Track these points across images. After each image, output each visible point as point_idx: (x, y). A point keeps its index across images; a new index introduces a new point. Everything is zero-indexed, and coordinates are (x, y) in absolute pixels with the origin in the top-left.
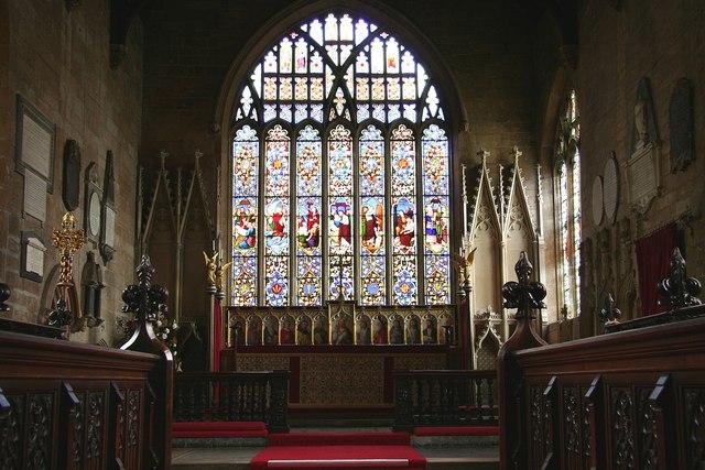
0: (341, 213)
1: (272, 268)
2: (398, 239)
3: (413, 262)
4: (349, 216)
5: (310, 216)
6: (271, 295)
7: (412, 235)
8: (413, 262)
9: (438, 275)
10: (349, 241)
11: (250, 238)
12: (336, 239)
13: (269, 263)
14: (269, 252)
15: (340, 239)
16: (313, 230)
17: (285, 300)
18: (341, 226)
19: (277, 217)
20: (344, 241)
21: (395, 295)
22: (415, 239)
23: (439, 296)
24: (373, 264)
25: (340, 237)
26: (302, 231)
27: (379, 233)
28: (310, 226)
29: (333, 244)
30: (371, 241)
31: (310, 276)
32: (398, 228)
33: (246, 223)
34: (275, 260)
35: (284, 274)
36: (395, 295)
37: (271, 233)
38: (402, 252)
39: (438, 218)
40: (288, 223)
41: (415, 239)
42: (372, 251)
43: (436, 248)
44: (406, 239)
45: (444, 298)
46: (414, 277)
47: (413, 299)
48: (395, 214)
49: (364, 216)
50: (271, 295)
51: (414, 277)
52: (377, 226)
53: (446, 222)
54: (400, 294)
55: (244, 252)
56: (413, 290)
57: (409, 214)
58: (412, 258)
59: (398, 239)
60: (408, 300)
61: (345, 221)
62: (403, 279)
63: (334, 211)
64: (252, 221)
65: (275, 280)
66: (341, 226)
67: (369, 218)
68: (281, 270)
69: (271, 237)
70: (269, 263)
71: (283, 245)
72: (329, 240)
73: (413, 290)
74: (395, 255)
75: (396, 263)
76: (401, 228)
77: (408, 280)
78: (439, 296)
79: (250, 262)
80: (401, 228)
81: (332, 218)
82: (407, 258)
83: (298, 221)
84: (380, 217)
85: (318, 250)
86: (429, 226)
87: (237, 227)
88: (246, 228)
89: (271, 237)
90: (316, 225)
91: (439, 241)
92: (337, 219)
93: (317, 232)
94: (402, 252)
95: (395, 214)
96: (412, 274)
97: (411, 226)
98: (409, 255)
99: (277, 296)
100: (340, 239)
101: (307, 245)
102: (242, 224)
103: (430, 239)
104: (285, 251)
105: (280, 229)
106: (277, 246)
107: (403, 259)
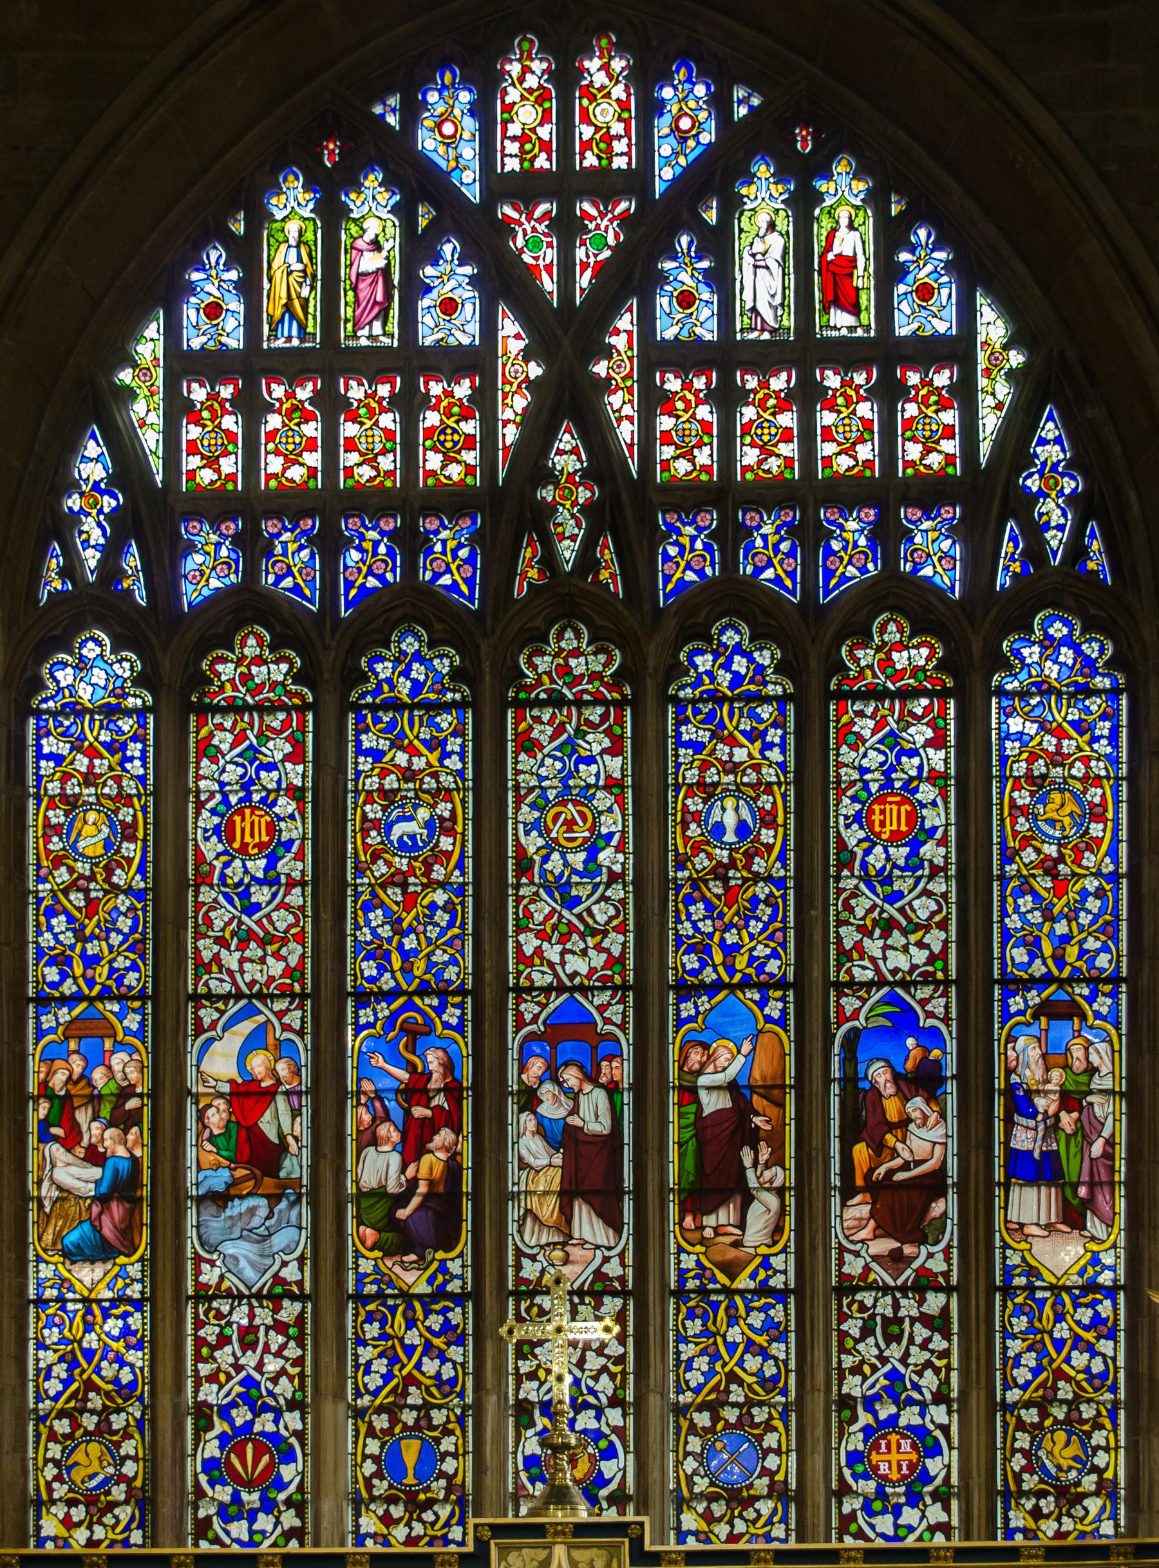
0: (571, 1077)
1: (224, 1356)
2: (858, 1209)
3: (938, 1323)
4: (612, 1089)
5: (417, 1090)
6: (224, 1494)
7: (934, 1184)
8: (938, 1323)
9: (1065, 1391)
10: (614, 1222)
11: (117, 1210)
12: (548, 1209)
13: (210, 1333)
14: (210, 1276)
15: (566, 1213)
16: (432, 1164)
17: (290, 1519)
18: (564, 1138)
19: (248, 1096)
20: (587, 1225)
21: (844, 1490)
22: (946, 1206)
23: (1069, 1497)
24: (735, 1334)
25: (567, 1196)
26: (379, 1167)
27: (767, 1176)
28: (413, 1146)
29: (532, 1237)
30: (725, 1216)
31: (415, 1397)
32: (861, 1152)
33: (92, 1130)
34: (240, 1316)
35: (285, 1388)
36: (844, 1490)
37: (219, 1180)
38: (879, 1274)
39: (1070, 1100)
40: (302, 1127)
41: (946, 1206)
42: (731, 1269)
43: (1062, 1256)
44: (903, 1208)
45: (1094, 1505)
46: (940, 1397)
47: (936, 1513)
48: (850, 1081)
49: (689, 1094)
50: (224, 1494)
51: (940, 1397)
52: (753, 1138)
53: (1110, 1115)
54: (870, 1486)
55: (87, 1275)
56: (934, 1466)
57: (923, 1081)
58: (934, 1302)
59: (858, 1209)
60: (910, 1516)
61: (594, 1114)
62: (886, 1410)
63: (536, 1067)
64: (123, 1120)
65: (241, 1415)
66: (564, 1138)
67: (713, 1103)
68: (272, 1365)
69: (220, 1199)
70: (210, 1333)
71: (280, 1240)
72: (513, 1213)
73: (934, 1466)
74: (847, 1287)
75: (853, 1327)
76: (879, 1150)
77: (910, 1417)
78: (1069, 1497)
79: (113, 1326)
80: (879, 1150)
81: (529, 1100)
82: (908, 1306)
83: (356, 1116)
84: (773, 1091)
85: (457, 1264)
86: (1025, 1139)
87: (56, 1150)
88: (95, 1157)
89: (220, 1199)
90: (445, 1136)
91: (1073, 1217)
92: (552, 1108)
93: (453, 1168)
94: (879, 1274)
95: (850, 1081)
96: (930, 1381)
97: (928, 1138)
98: (924, 1283)
99: (252, 1498)
100: (566, 1213)
101: (400, 1240)
102: (71, 1141)
103: (1029, 1204)
104: (291, 1273)
105: (258, 1156)
106: (248, 1249)
107: (885, 1306)
